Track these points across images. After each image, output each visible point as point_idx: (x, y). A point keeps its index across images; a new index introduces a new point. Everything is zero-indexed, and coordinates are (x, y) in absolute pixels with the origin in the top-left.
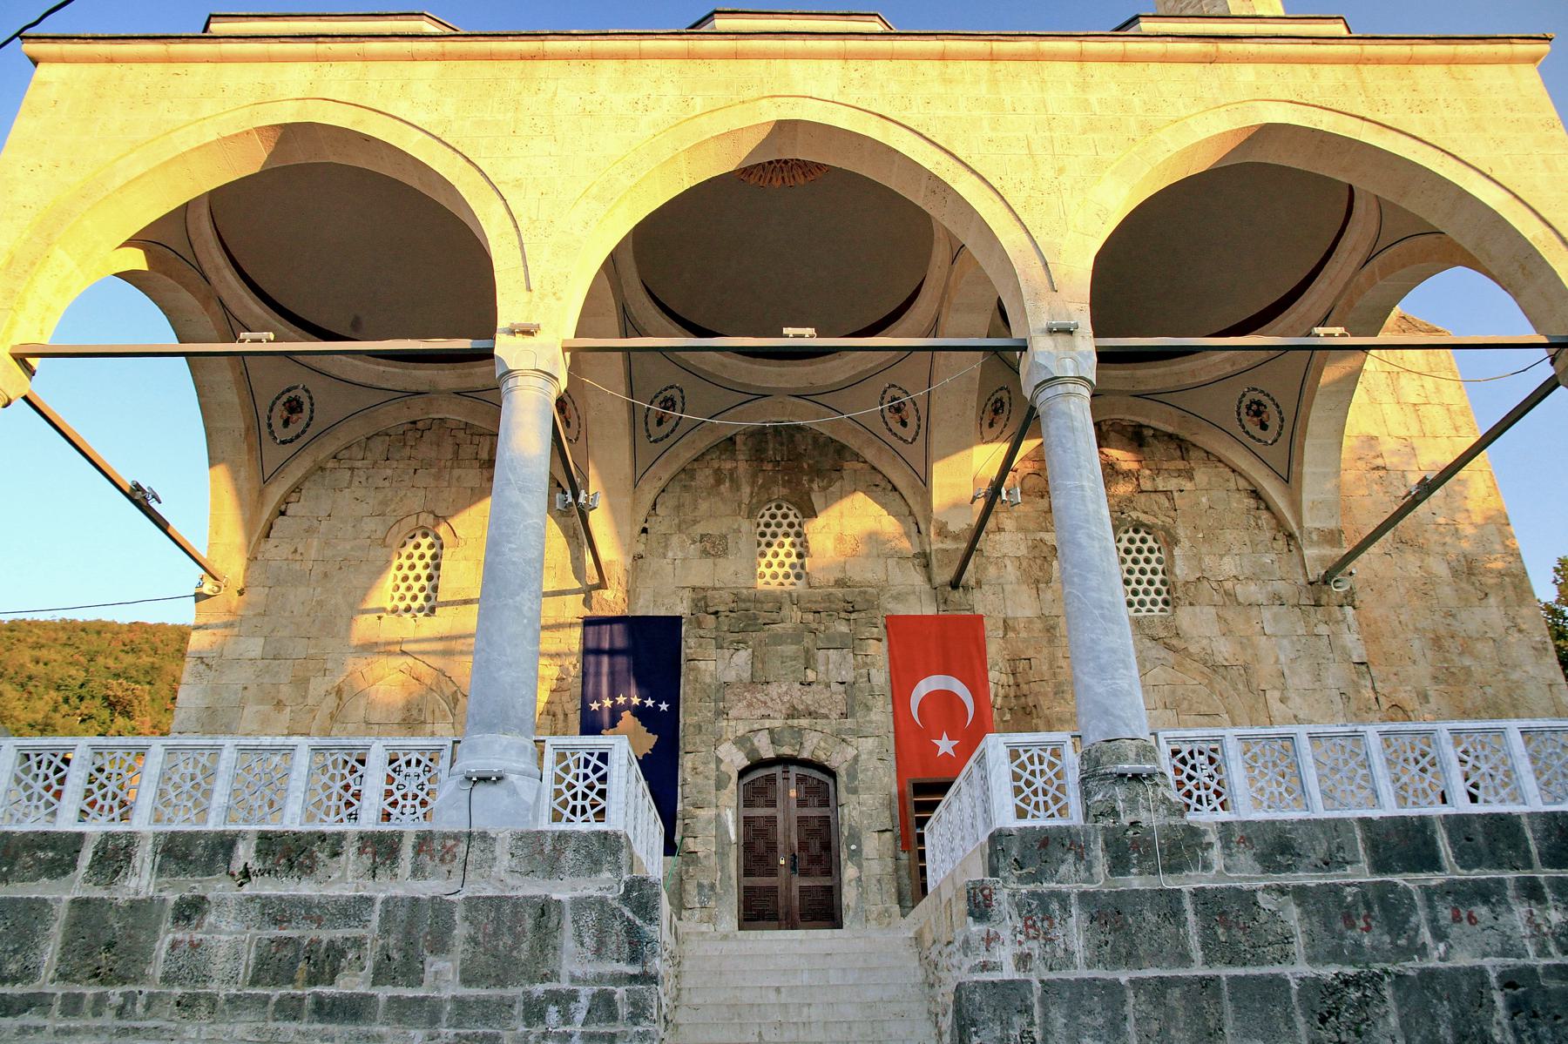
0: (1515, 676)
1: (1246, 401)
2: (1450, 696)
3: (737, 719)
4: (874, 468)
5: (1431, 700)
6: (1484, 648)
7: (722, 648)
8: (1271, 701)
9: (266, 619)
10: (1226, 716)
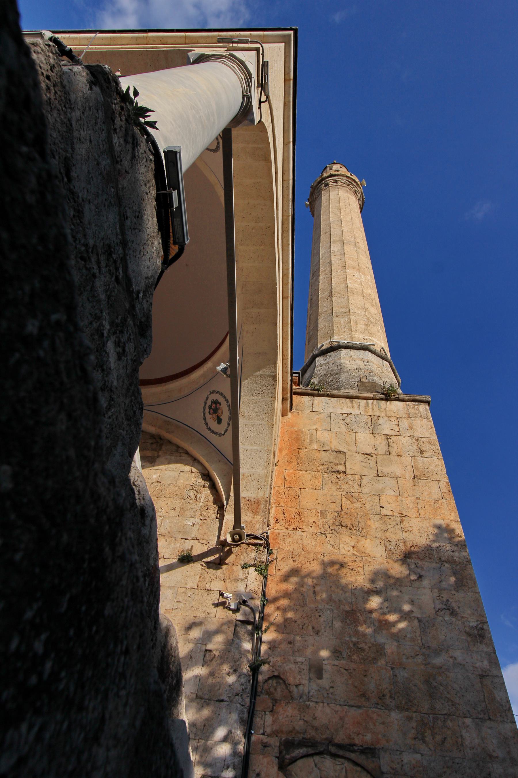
0: (437, 661)
1: (209, 403)
5: (325, 676)
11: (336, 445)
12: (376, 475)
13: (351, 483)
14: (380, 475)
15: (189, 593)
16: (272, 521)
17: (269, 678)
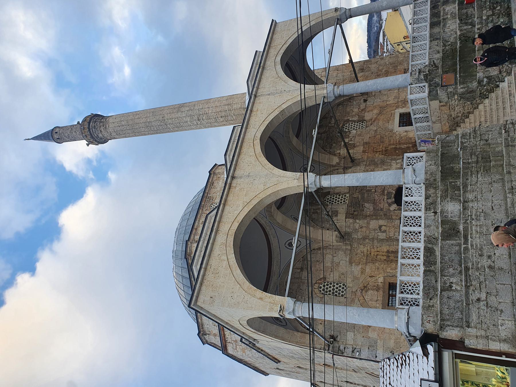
3: (384, 206)
6: (381, 68)
7: (364, 210)
8: (389, 103)
9: (342, 331)
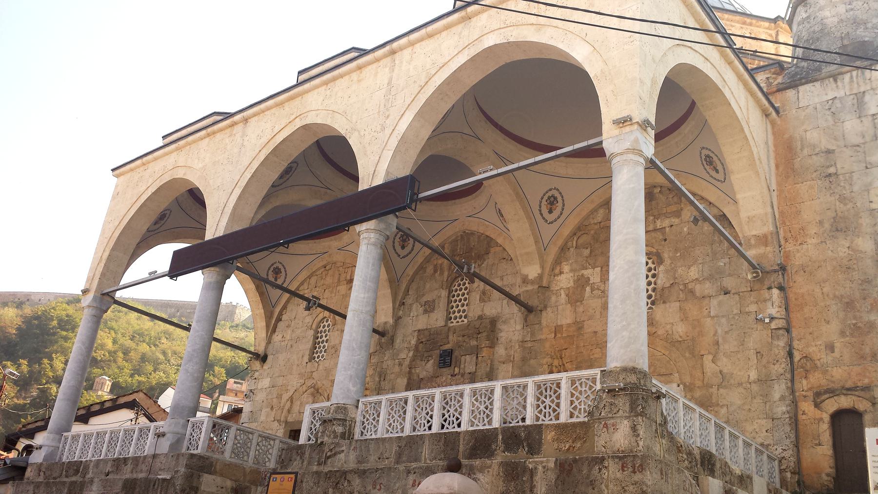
2: (853, 346)
4: (504, 249)
5: (836, 350)
10: (676, 375)
11: (825, 143)
12: (864, 168)
13: (842, 184)
14: (869, 166)
15: (737, 318)
16: (783, 242)
17: (801, 359)
